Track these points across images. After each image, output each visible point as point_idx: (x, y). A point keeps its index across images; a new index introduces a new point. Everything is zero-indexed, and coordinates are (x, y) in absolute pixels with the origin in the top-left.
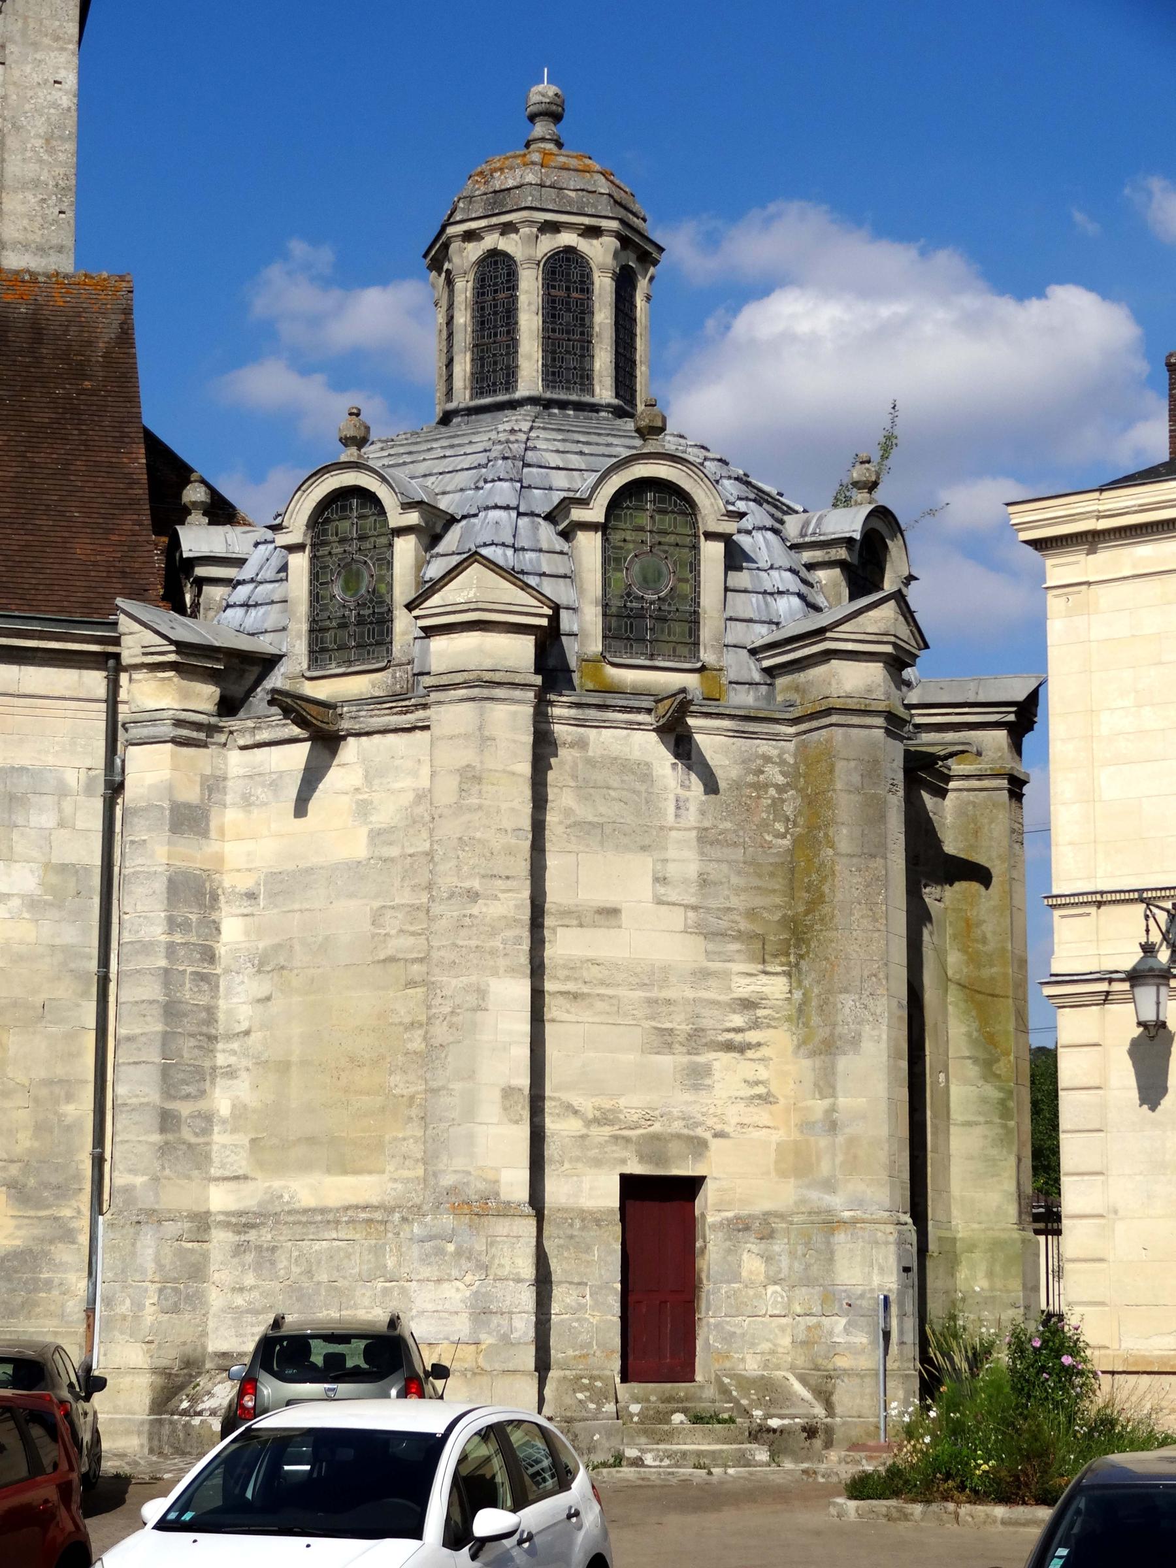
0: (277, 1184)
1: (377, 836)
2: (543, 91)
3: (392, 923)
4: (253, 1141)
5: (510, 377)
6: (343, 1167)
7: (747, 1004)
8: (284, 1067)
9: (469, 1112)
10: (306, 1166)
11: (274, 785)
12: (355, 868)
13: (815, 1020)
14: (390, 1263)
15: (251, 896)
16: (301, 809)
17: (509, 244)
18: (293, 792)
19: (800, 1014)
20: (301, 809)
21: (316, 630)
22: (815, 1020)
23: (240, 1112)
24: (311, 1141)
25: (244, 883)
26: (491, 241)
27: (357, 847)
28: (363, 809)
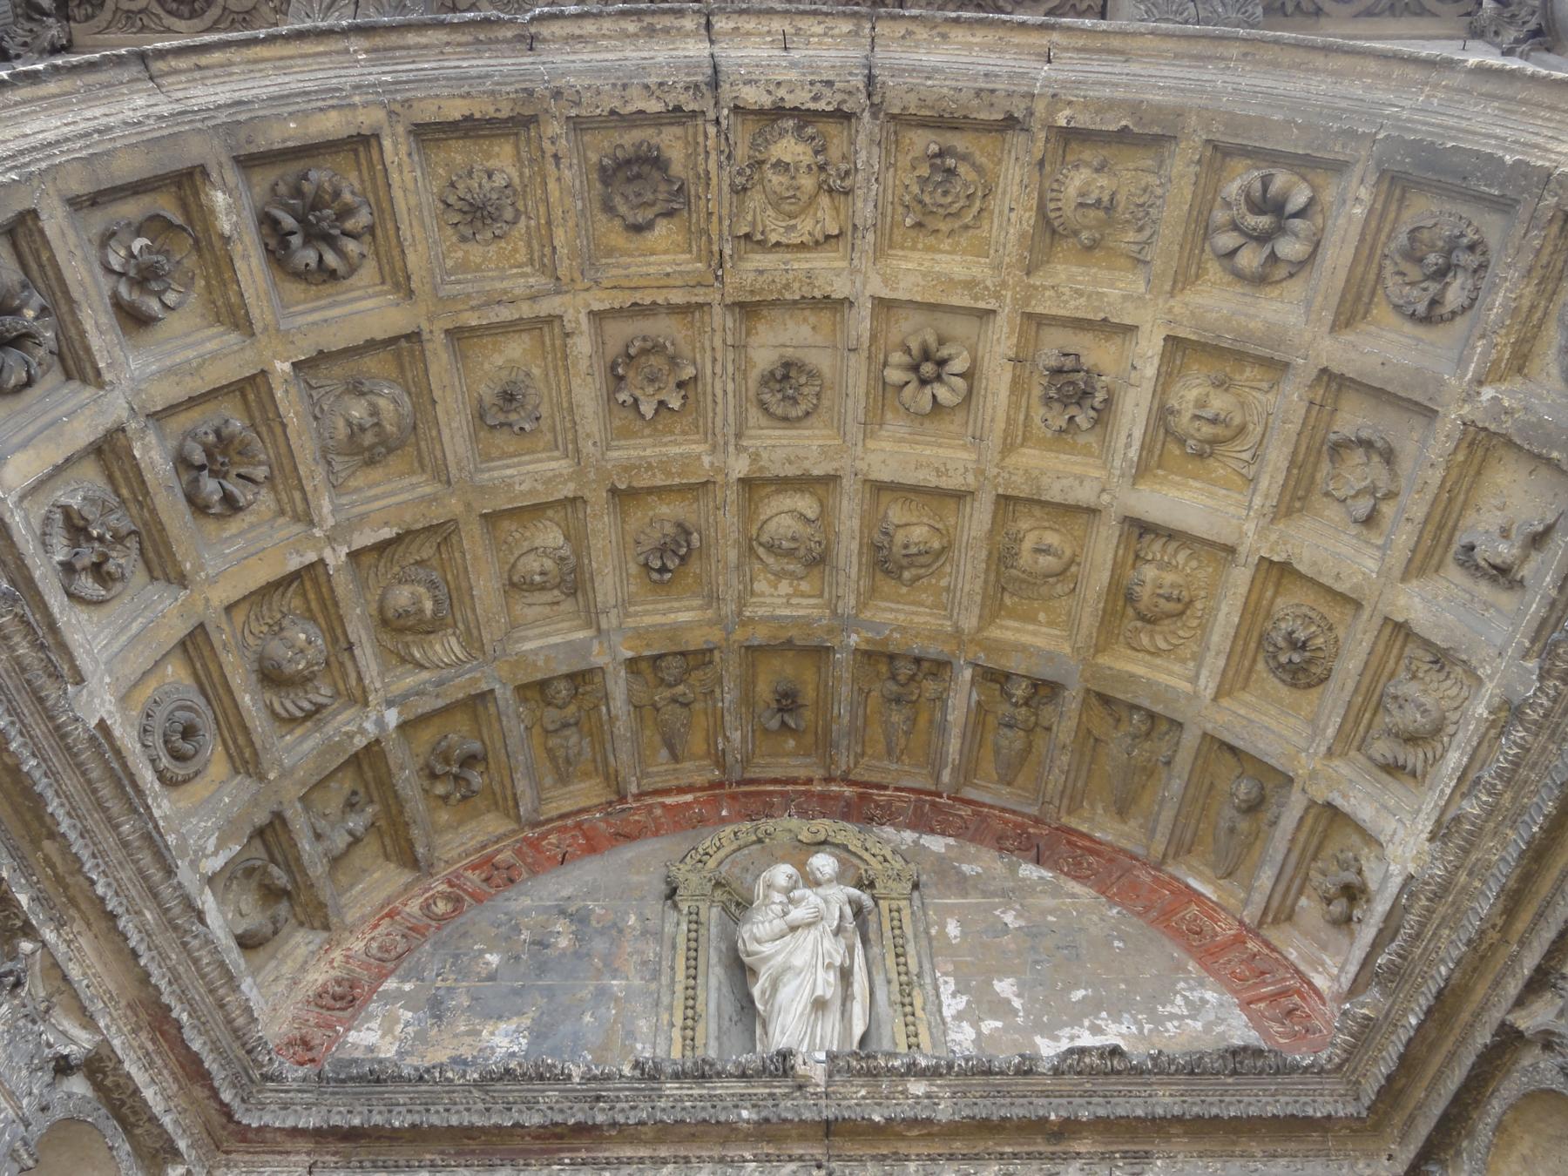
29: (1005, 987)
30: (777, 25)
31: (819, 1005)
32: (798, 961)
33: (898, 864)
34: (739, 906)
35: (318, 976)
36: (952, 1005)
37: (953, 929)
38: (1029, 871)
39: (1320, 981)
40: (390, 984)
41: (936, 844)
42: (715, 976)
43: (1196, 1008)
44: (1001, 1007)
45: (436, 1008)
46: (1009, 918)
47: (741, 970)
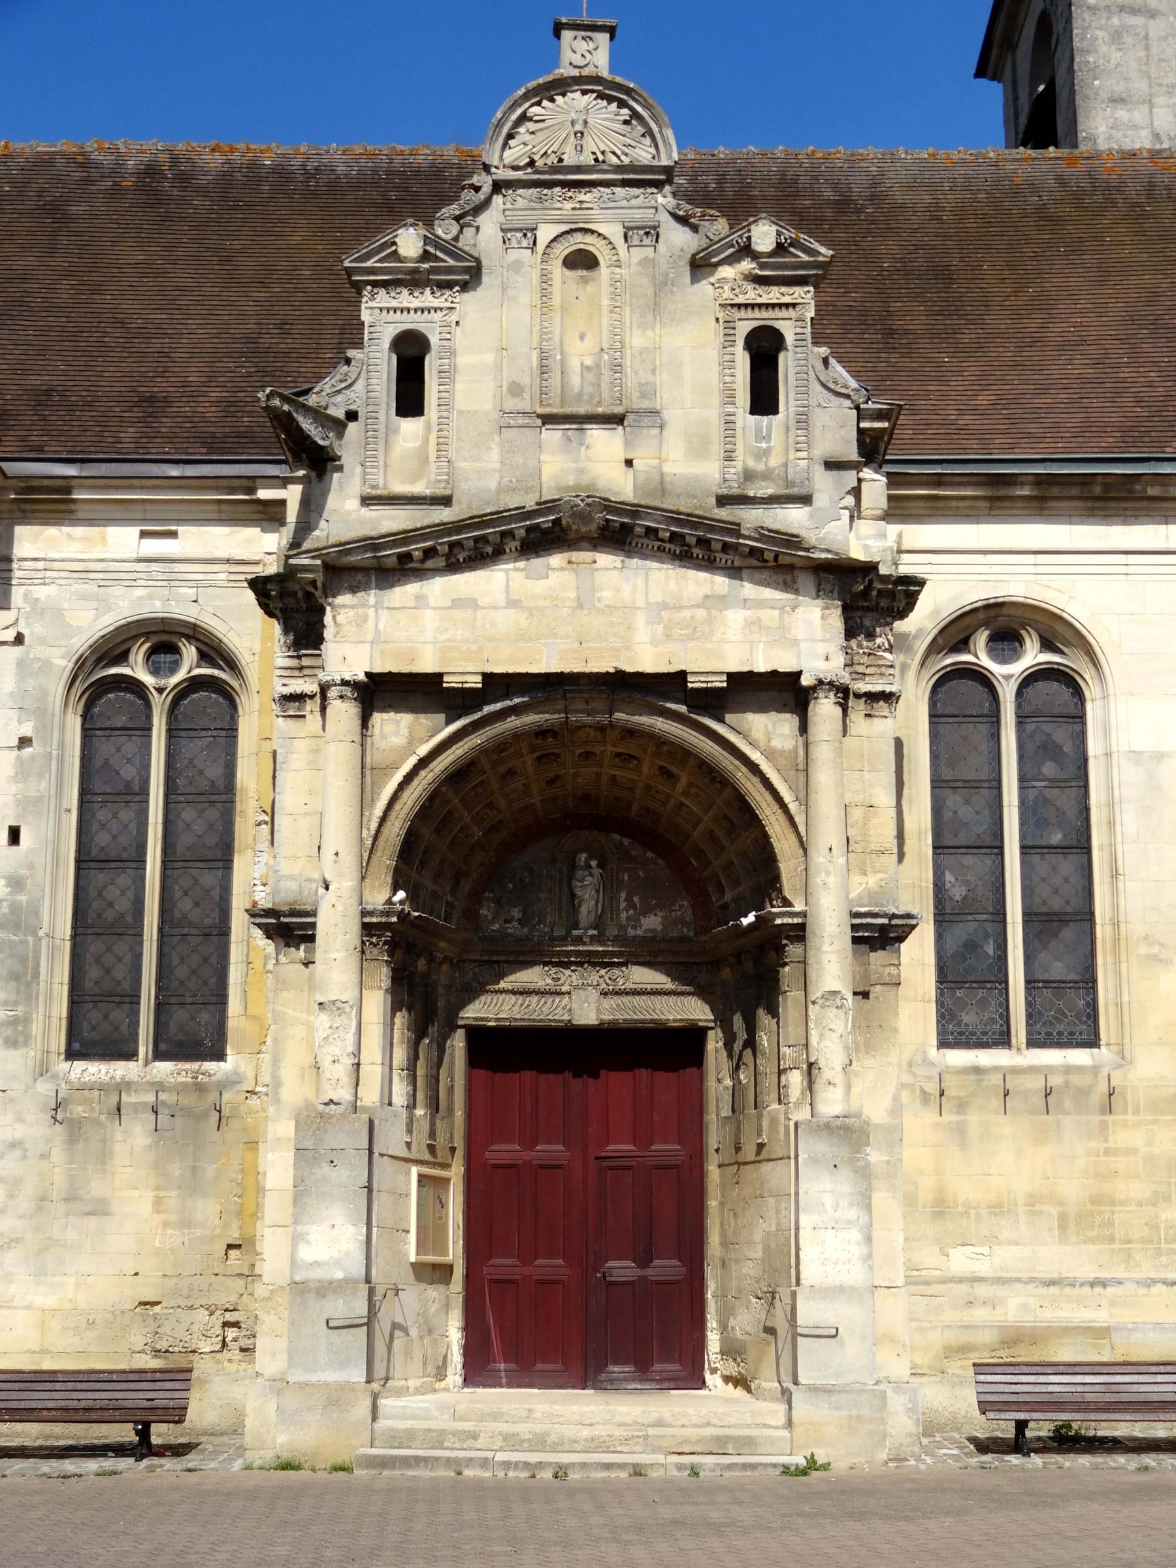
29: (636, 899)
30: (586, 695)
31: (589, 912)
32: (586, 897)
33: (614, 850)
34: (573, 866)
35: (467, 887)
36: (623, 905)
37: (626, 878)
38: (650, 854)
39: (714, 899)
40: (487, 894)
41: (626, 841)
42: (566, 890)
43: (681, 907)
44: (634, 906)
45: (498, 902)
46: (641, 874)
47: (573, 896)
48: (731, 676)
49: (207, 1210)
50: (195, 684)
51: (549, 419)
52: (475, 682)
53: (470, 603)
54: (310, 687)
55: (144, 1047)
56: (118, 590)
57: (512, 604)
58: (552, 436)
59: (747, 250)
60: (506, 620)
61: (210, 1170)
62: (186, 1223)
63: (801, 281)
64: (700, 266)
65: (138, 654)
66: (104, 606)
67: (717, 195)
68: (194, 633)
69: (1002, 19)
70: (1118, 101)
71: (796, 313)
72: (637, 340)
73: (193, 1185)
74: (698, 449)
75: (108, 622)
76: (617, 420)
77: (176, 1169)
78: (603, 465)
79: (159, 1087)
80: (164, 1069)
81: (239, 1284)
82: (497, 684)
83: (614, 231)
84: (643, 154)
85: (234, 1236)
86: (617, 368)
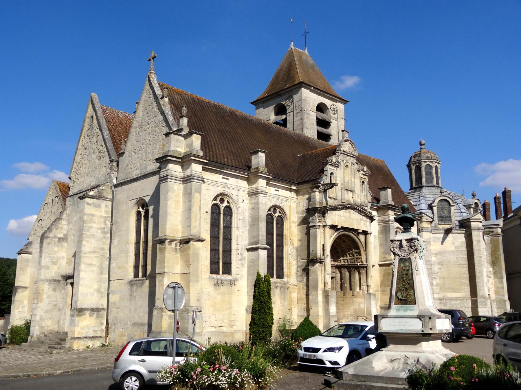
0: (445, 294)
1: (456, 247)
2: (423, 142)
3: (460, 259)
4: (440, 288)
5: (432, 182)
6: (455, 292)
7: (490, 272)
8: (444, 278)
9: (484, 286)
10: (449, 292)
11: (439, 239)
12: (453, 251)
13: (498, 274)
14: (465, 305)
15: (436, 254)
16: (442, 243)
17: (431, 164)
18: (441, 240)
19: (495, 273)
20: (442, 243)
21: (439, 217)
22: (498, 274)
23: (437, 285)
24: (450, 288)
25: (435, 252)
26: (428, 163)
27: (453, 248)
28: (453, 244)
48: (363, 231)
49: (286, 303)
50: (279, 216)
51: (346, 190)
52: (340, 227)
53: (339, 215)
54: (321, 224)
55: (275, 277)
56: (272, 199)
57: (344, 216)
58: (346, 192)
59: (363, 170)
60: (343, 219)
61: (286, 297)
62: (284, 306)
63: (366, 175)
64: (359, 171)
65: (272, 210)
66: (271, 202)
67: (360, 160)
68: (280, 207)
69: (266, 99)
70: (307, 128)
71: (366, 181)
72: (353, 180)
73: (284, 299)
74: (358, 197)
75: (271, 205)
76: (352, 191)
77: (283, 297)
78: (349, 198)
79: (280, 283)
80: (278, 279)
81: (290, 315)
82: (343, 228)
83: (350, 163)
84: (353, 153)
85: (289, 308)
86: (351, 183)
